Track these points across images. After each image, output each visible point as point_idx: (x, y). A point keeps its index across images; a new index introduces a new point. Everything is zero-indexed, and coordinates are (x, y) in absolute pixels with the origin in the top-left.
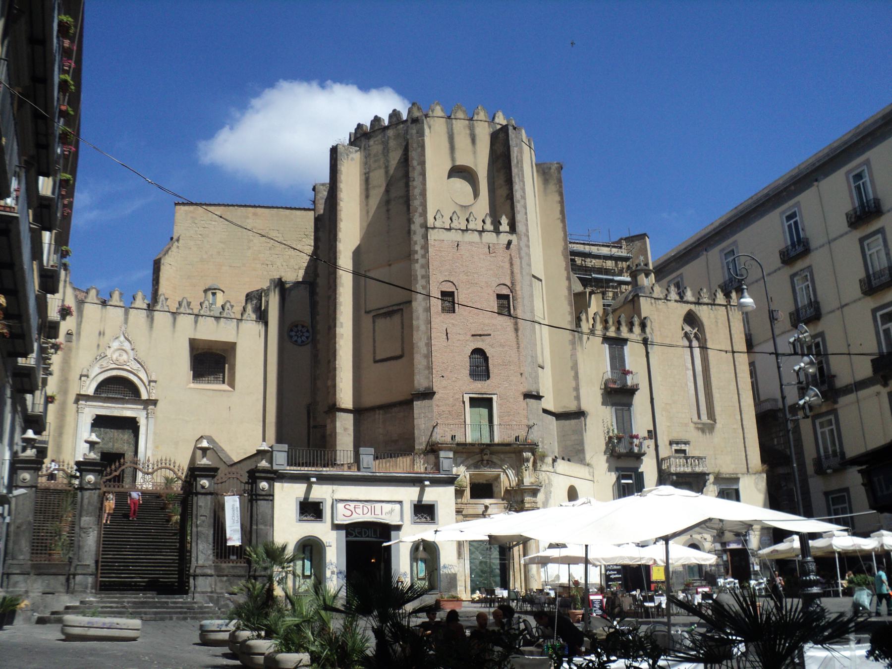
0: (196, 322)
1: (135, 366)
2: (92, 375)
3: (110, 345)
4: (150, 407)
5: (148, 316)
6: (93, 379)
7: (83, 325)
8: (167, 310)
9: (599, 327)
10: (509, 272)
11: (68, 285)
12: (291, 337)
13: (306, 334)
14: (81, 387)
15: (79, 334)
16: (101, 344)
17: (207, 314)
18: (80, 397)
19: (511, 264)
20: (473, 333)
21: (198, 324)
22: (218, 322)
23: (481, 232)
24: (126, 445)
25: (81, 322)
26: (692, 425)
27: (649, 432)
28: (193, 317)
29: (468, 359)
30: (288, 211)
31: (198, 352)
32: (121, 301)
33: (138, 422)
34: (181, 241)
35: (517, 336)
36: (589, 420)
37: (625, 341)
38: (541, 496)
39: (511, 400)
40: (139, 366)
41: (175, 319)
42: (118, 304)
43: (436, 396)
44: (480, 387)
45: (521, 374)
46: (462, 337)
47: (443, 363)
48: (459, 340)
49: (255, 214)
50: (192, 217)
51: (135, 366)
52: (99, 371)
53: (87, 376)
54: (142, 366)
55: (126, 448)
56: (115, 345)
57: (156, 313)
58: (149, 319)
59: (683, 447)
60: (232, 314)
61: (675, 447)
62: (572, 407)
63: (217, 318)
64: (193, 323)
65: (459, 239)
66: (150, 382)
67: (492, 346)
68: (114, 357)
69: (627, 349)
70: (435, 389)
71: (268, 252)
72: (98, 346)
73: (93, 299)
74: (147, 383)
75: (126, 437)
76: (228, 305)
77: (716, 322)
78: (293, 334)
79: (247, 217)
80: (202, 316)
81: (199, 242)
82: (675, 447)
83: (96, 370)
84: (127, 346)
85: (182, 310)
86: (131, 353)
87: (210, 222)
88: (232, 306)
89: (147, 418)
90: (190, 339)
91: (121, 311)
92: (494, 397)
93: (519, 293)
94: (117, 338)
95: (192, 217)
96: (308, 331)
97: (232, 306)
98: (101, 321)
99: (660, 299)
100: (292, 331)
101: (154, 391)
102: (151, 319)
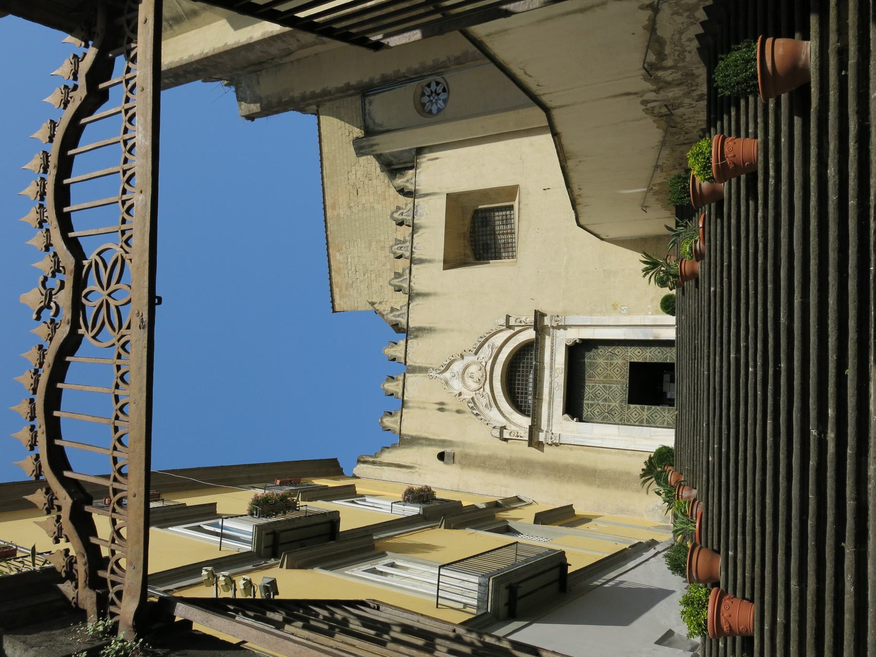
0: (421, 261)
1: (486, 352)
2: (502, 421)
3: (457, 392)
4: (547, 321)
5: (416, 337)
6: (507, 419)
7: (431, 436)
8: (406, 307)
11: (378, 459)
12: (439, 110)
13: (433, 87)
14: (518, 439)
15: (443, 443)
16: (455, 408)
17: (408, 244)
18: (533, 441)
21: (424, 257)
22: (420, 227)
24: (615, 362)
25: (427, 439)
28: (414, 267)
30: (325, 163)
31: (469, 252)
32: (397, 380)
34: (374, 300)
40: (486, 345)
41: (419, 295)
42: (401, 383)
49: (334, 208)
50: (347, 289)
51: (486, 352)
52: (495, 410)
54: (487, 340)
55: (620, 362)
57: (411, 325)
58: (420, 334)
60: (408, 208)
63: (415, 228)
64: (423, 265)
66: (509, 327)
68: (475, 386)
71: (374, 181)
72: (458, 412)
73: (395, 422)
74: (511, 332)
75: (601, 361)
76: (396, 215)
78: (434, 109)
79: (338, 215)
80: (412, 252)
81: (373, 275)
83: (494, 414)
84: (457, 367)
85: (406, 285)
86: (469, 359)
87: (349, 264)
88: (398, 208)
89: (565, 327)
90: (445, 269)
91: (411, 378)
94: (447, 383)
95: (347, 289)
96: (429, 85)
97: (398, 208)
98: (424, 408)
100: (430, 112)
101: (523, 319)
102: (421, 331)
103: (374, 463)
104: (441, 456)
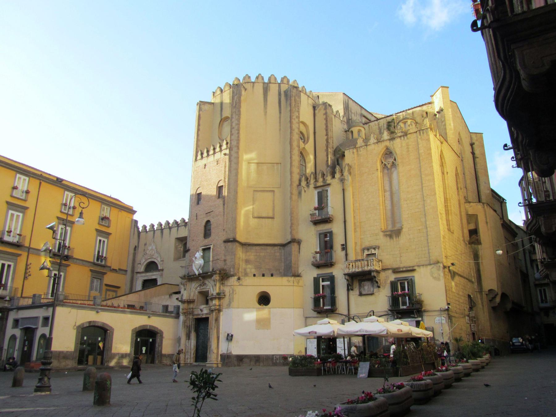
1: (156, 255)
2: (142, 262)
5: (161, 232)
9: (312, 181)
10: (224, 172)
19: (225, 167)
20: (206, 213)
21: (179, 231)
26: (382, 234)
27: (342, 245)
28: (176, 228)
29: (203, 228)
33: (157, 281)
35: (224, 208)
36: (302, 245)
37: (329, 185)
38: (225, 302)
39: (218, 246)
41: (170, 231)
43: (190, 251)
45: (224, 230)
47: (194, 233)
48: (201, 218)
53: (140, 264)
56: (150, 248)
59: (373, 251)
61: (366, 252)
65: (205, 163)
67: (213, 218)
68: (150, 253)
77: (408, 148)
83: (144, 260)
92: (212, 246)
99: (361, 147)
103: (135, 226)
104: (136, 246)
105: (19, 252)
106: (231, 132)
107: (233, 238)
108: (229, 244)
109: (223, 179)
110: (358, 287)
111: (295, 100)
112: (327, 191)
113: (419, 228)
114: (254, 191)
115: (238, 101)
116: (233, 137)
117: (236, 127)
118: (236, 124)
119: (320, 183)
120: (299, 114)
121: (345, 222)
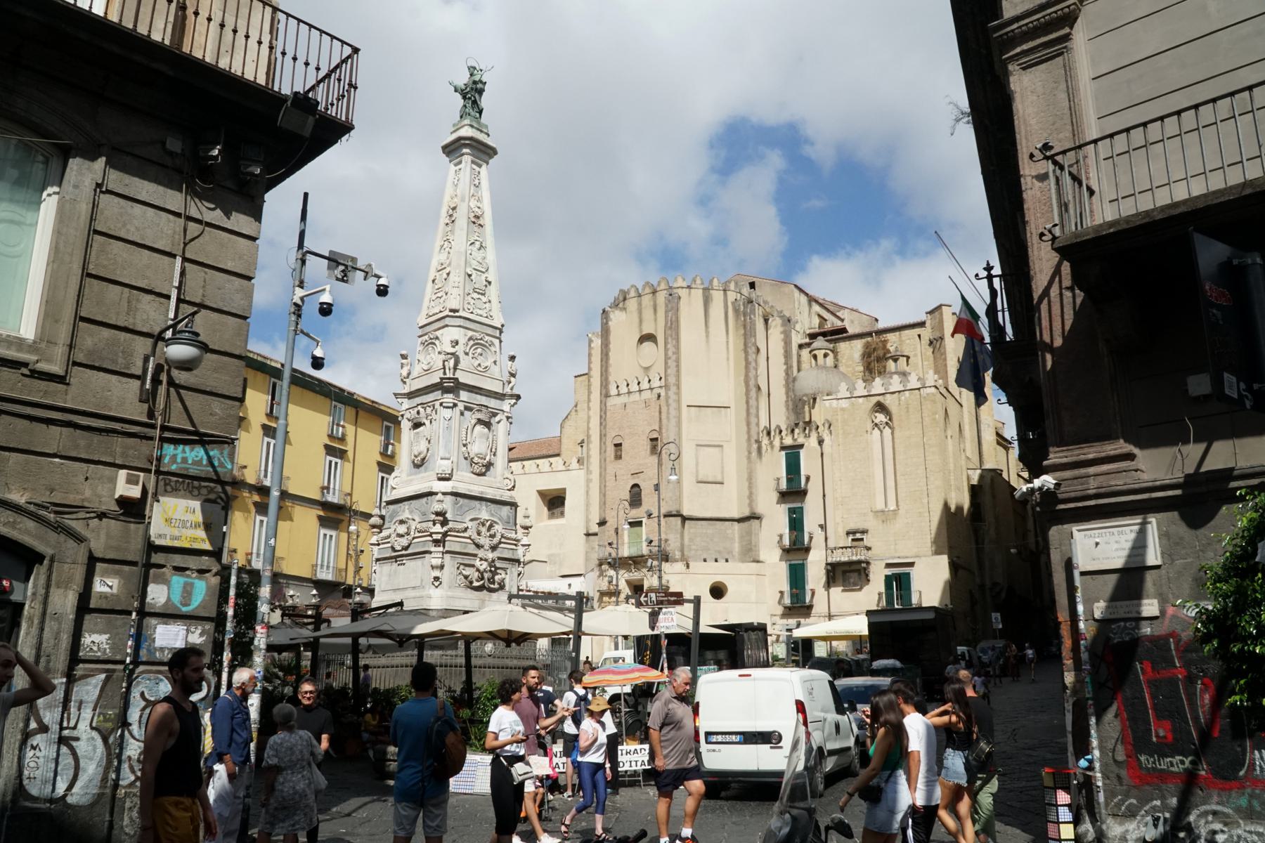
10: (658, 419)
19: (660, 412)
23: (640, 391)
26: (871, 514)
37: (801, 446)
43: (608, 524)
44: (635, 514)
46: (625, 478)
62: (747, 513)
67: (644, 481)
69: (802, 453)
70: (607, 519)
77: (907, 408)
82: (851, 537)
93: (664, 435)
105: (341, 517)
106: (666, 363)
107: (677, 511)
108: (672, 519)
109: (657, 429)
110: (841, 581)
111: (750, 318)
112: (799, 452)
113: (920, 510)
114: (698, 445)
115: (674, 319)
116: (669, 371)
117: (674, 357)
118: (674, 353)
119: (788, 441)
120: (755, 340)
121: (824, 496)
